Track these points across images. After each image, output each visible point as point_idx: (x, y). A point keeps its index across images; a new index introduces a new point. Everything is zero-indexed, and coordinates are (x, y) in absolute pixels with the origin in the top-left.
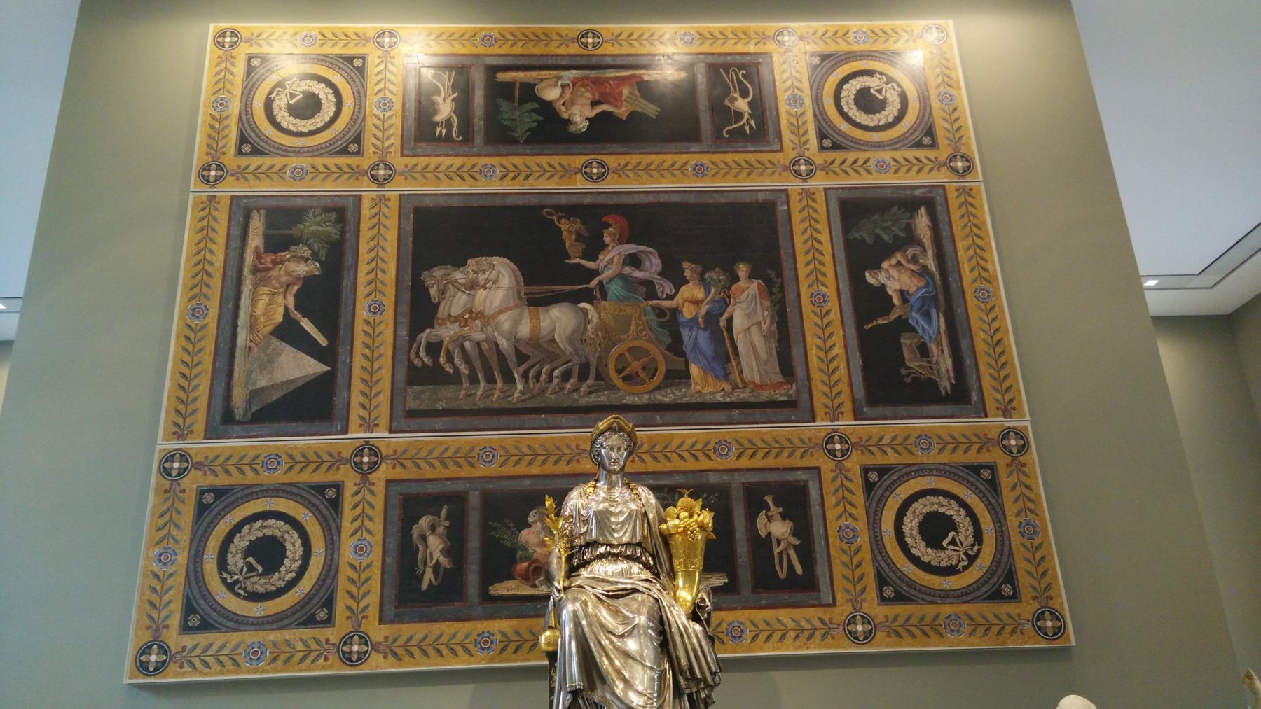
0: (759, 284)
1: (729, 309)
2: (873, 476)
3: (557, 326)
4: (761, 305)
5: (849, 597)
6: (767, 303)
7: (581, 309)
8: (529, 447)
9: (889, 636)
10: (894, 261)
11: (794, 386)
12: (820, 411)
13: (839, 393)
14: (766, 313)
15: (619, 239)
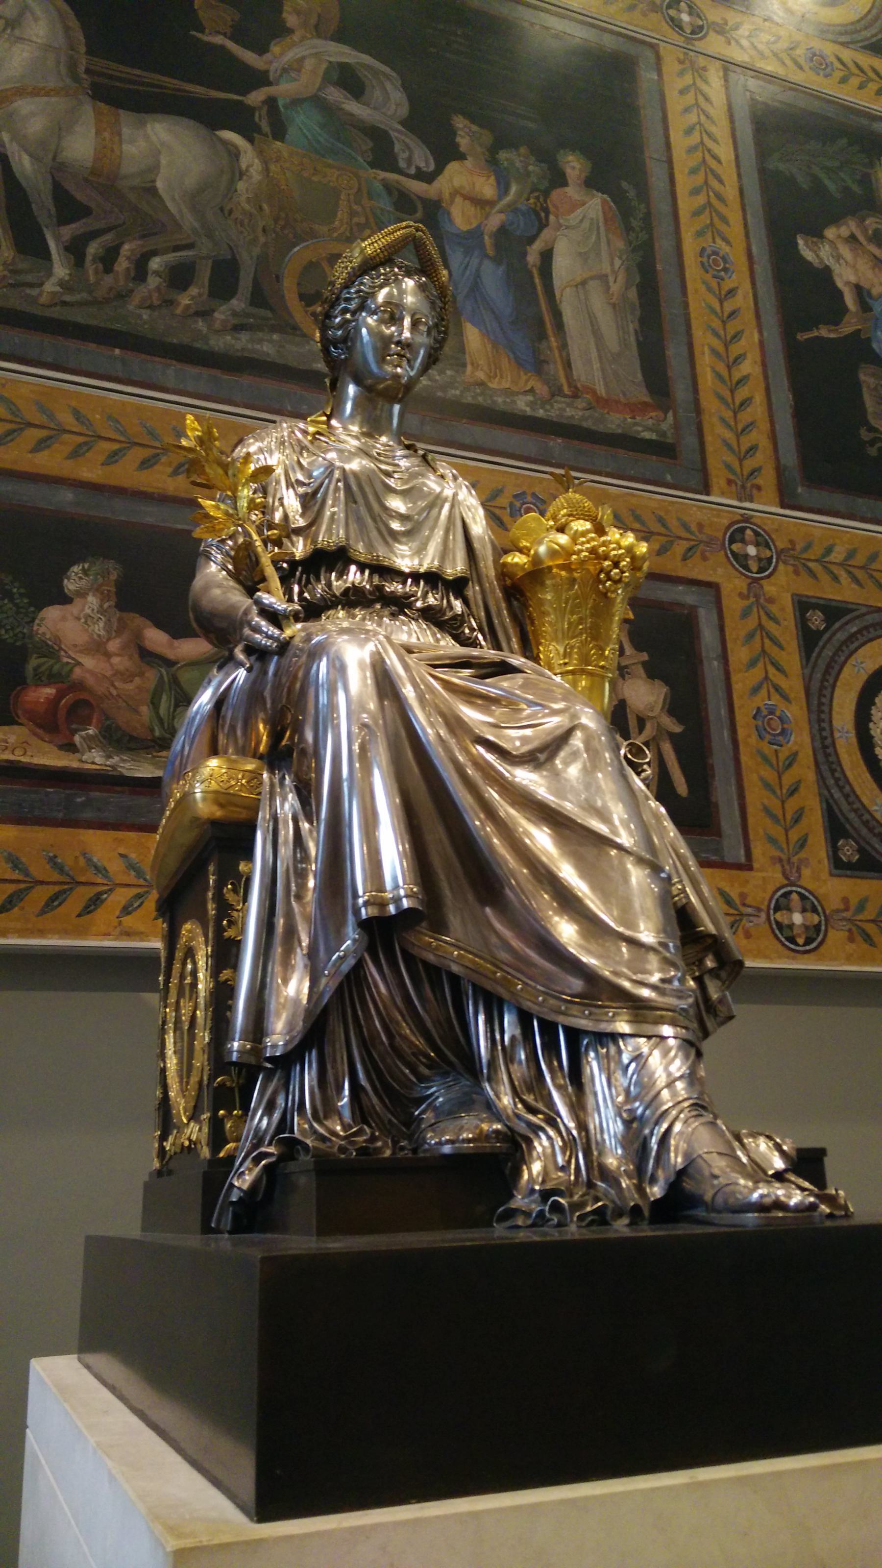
0: (604, 202)
1: (546, 234)
2: (816, 620)
3: (163, 161)
4: (609, 243)
5: (777, 853)
6: (620, 244)
7: (225, 143)
8: (77, 414)
9: (851, 939)
10: (844, 231)
11: (670, 414)
12: (718, 477)
13: (753, 449)
14: (618, 262)
15: (316, 27)
